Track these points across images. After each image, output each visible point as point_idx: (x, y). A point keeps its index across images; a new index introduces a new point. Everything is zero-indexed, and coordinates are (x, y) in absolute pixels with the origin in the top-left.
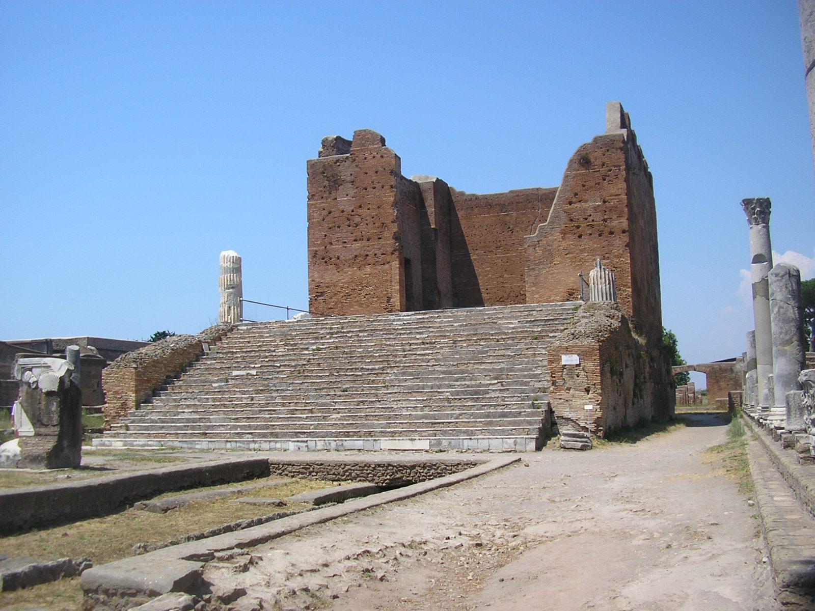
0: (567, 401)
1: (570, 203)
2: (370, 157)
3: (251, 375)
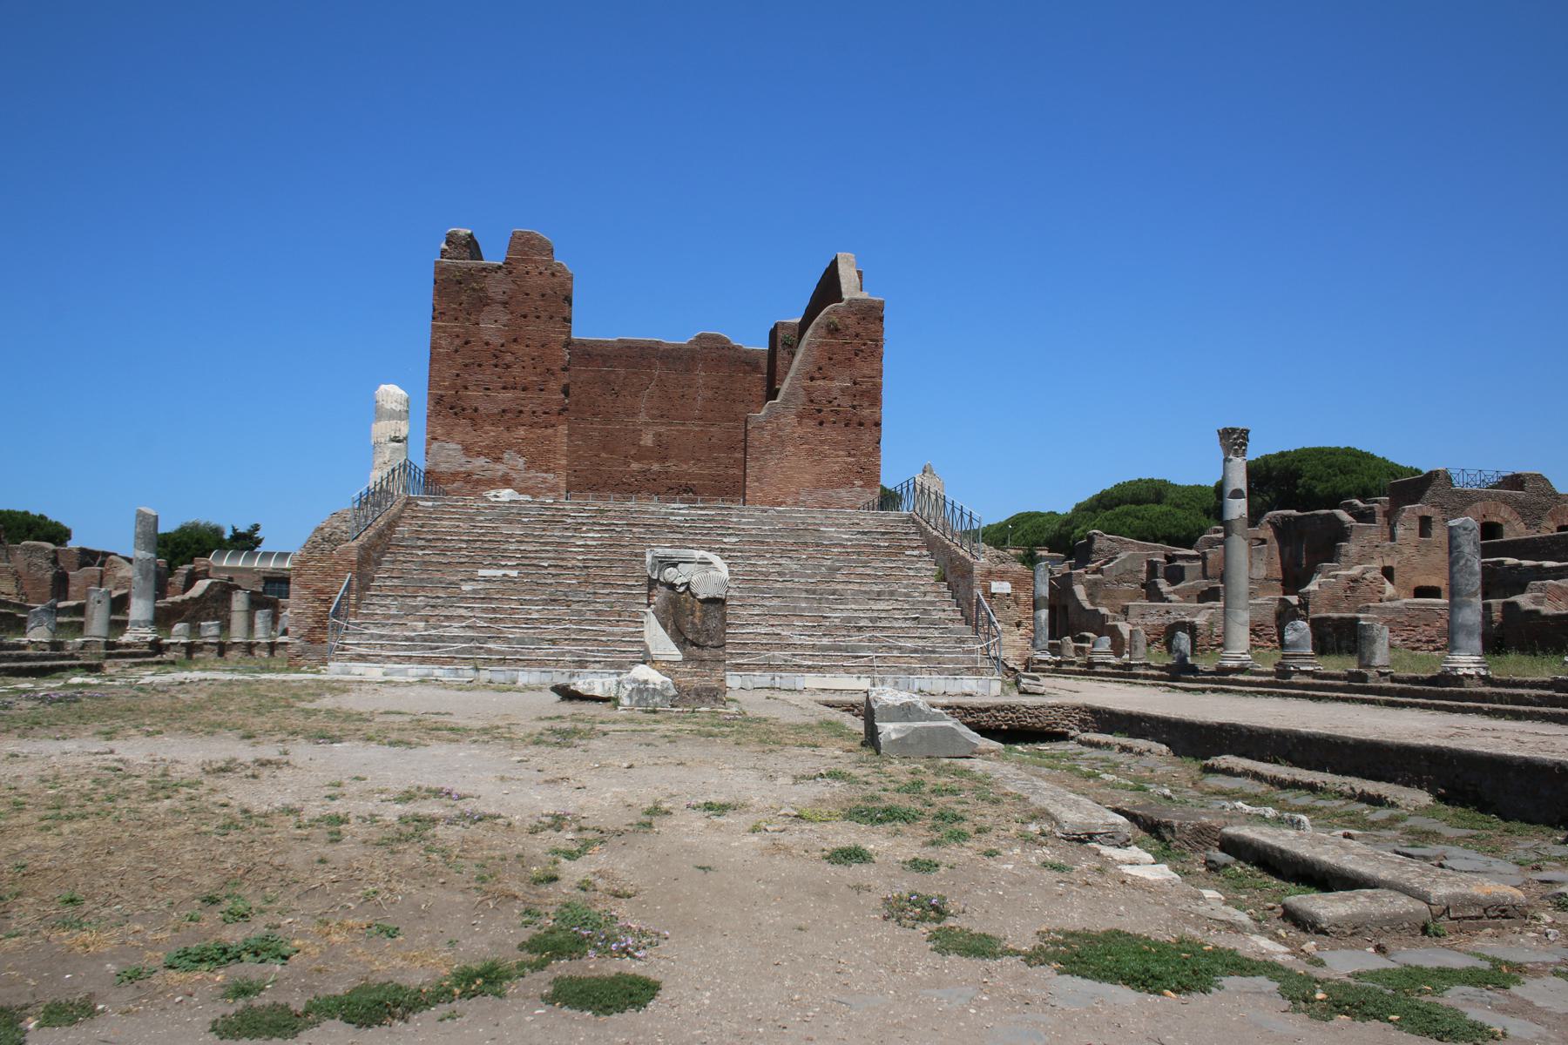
1: (812, 379)
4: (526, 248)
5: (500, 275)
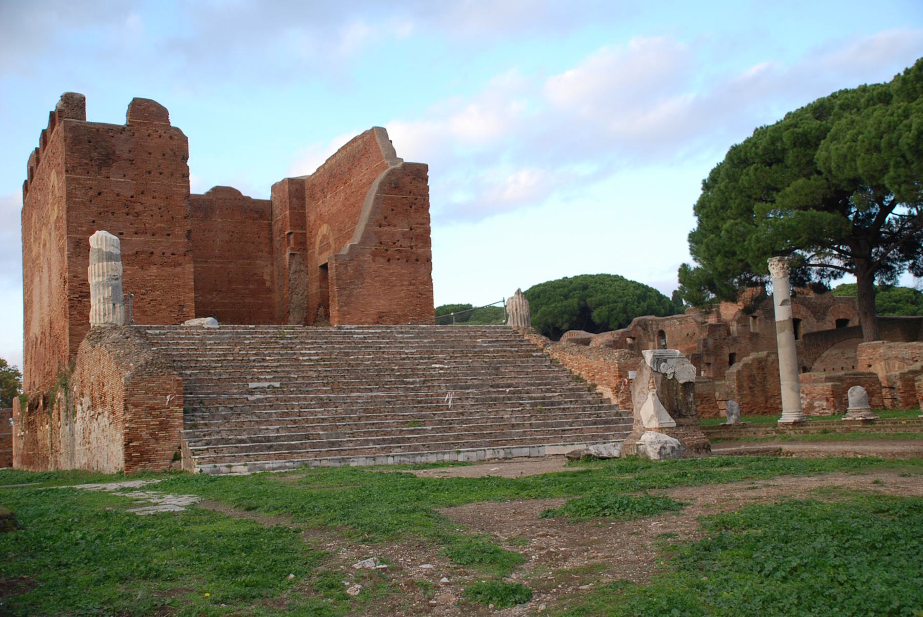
2: (156, 135)
3: (274, 387)
4: (146, 113)
5: (123, 136)
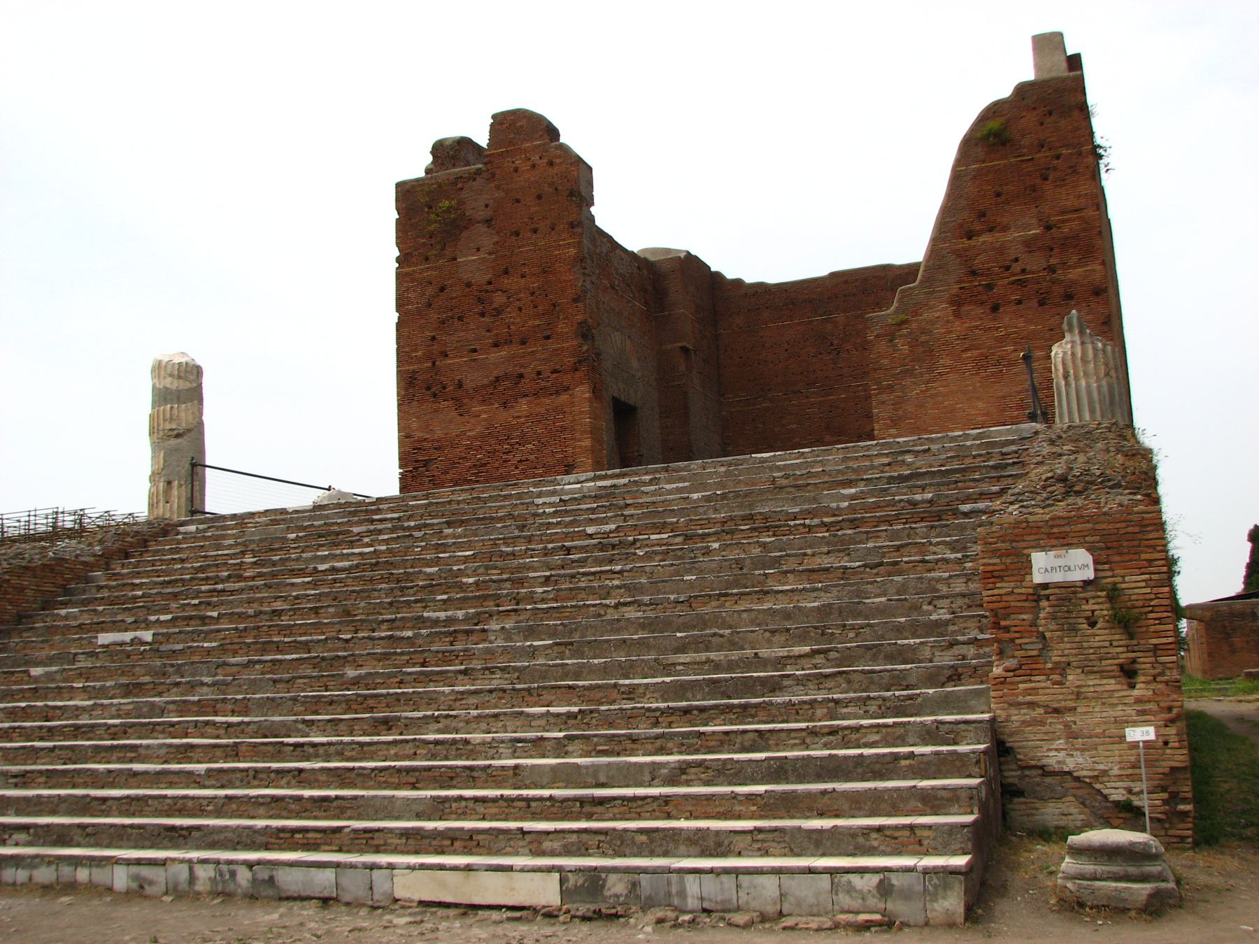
0: (1056, 711)
1: (970, 238)
2: (525, 167)
